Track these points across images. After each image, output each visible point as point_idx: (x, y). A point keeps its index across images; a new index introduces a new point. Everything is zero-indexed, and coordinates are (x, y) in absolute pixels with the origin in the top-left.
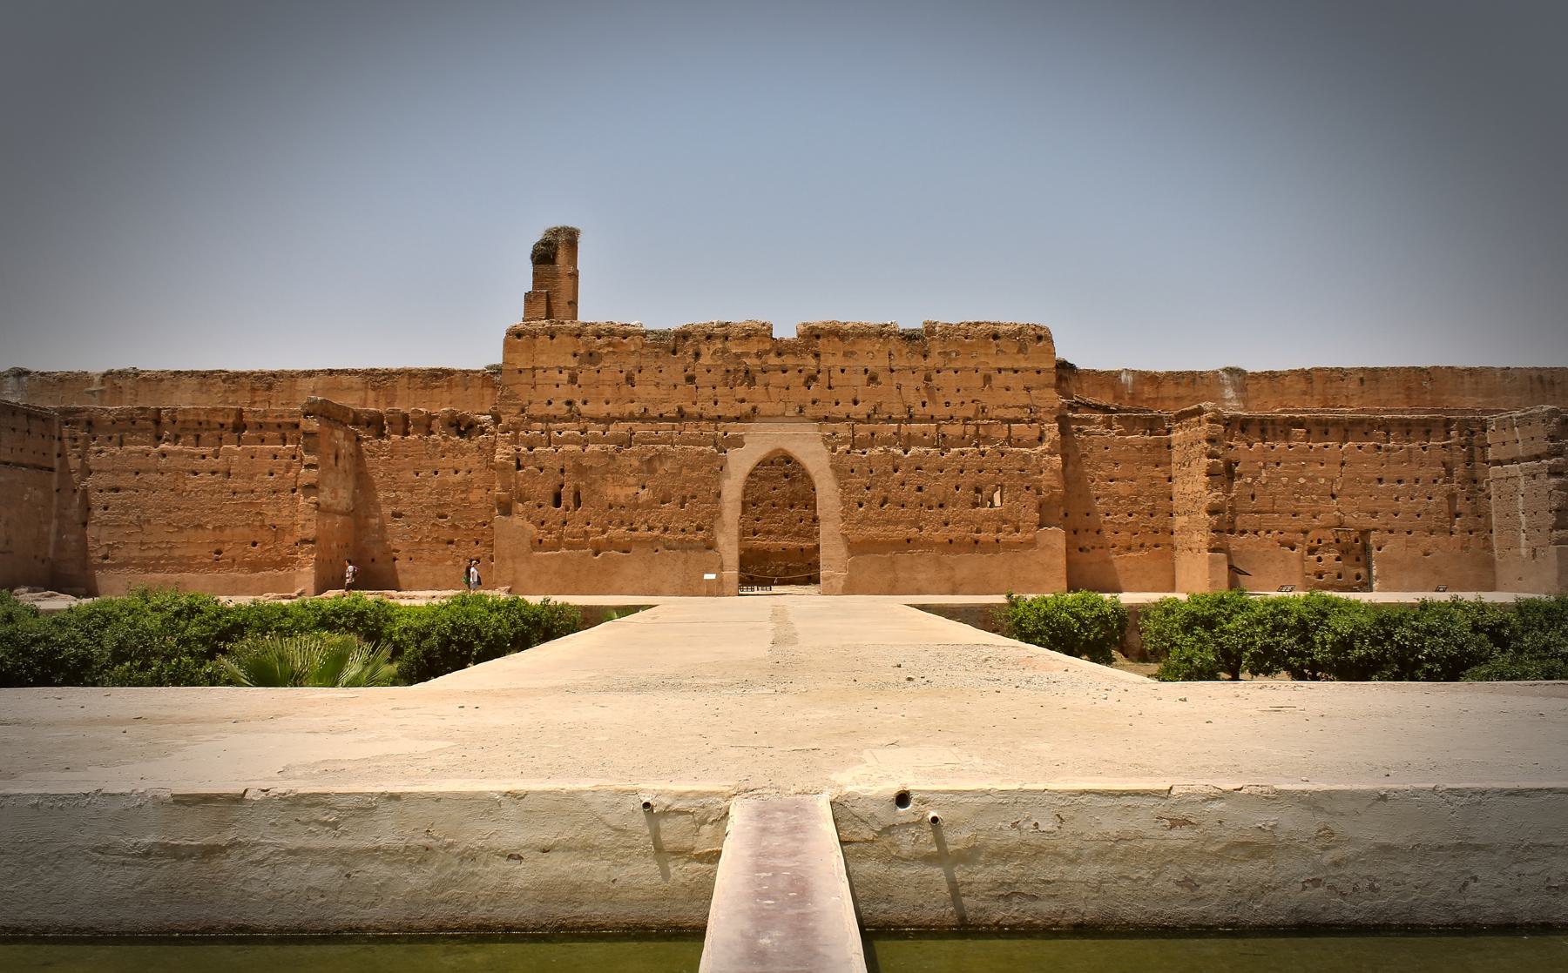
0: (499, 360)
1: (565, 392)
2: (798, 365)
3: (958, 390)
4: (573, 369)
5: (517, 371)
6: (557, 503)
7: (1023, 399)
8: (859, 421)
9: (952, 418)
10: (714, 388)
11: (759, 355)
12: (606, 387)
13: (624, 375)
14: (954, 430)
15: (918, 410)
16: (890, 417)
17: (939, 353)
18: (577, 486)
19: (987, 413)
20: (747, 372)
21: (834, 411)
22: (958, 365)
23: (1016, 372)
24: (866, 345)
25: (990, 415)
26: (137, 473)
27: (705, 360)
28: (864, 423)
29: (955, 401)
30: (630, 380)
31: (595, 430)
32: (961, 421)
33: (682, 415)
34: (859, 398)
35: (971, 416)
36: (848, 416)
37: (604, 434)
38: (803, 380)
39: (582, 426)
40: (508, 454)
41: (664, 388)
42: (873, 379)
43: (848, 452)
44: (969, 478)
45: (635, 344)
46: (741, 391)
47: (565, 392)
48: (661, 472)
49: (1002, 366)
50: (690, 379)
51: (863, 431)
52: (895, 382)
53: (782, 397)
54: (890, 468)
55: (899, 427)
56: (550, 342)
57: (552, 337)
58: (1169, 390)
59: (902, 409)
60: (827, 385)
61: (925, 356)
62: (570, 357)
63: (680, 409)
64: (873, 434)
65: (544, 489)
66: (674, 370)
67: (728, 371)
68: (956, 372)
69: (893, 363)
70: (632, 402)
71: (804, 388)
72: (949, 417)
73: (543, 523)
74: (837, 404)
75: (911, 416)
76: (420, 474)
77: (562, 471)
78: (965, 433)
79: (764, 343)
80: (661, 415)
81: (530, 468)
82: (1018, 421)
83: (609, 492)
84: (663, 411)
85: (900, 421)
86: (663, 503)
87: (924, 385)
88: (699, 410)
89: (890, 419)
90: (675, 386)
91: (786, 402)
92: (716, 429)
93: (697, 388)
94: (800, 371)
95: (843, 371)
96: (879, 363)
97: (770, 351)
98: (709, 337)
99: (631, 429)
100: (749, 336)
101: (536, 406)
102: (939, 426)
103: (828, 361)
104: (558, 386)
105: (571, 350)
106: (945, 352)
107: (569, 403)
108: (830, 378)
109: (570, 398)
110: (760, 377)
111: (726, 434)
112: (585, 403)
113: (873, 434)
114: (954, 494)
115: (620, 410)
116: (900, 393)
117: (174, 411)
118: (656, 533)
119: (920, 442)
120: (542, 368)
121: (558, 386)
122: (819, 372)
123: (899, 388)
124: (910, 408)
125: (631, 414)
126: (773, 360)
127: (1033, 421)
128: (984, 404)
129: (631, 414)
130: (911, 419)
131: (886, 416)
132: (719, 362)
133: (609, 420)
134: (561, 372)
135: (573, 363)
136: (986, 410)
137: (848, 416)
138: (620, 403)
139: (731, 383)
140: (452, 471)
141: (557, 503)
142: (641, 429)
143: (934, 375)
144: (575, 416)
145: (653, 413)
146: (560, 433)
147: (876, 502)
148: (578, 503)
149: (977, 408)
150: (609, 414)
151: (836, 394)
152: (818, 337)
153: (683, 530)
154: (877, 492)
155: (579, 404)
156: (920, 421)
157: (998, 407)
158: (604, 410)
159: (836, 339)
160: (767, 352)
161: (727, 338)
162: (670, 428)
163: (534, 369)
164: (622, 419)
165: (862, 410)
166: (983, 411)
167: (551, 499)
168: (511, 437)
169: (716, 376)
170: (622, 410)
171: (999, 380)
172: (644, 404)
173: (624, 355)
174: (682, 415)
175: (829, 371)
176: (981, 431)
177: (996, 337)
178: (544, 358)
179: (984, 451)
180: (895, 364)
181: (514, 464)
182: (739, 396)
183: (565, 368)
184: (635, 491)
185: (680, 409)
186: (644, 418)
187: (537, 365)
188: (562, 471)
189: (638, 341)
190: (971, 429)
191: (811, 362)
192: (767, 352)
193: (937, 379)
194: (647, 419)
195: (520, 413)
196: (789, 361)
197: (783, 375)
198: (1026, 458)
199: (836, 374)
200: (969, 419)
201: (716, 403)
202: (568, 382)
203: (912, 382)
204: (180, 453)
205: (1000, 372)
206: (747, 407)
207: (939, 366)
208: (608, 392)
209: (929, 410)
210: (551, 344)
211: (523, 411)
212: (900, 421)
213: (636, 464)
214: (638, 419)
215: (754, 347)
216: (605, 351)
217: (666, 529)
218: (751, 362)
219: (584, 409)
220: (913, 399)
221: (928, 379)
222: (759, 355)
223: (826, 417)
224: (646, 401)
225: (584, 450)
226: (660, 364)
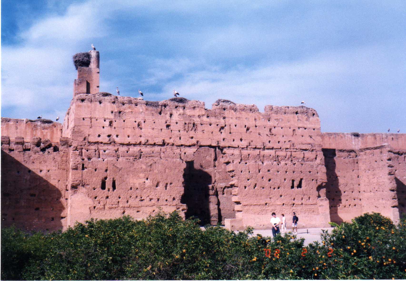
1: (107, 130)
3: (283, 136)
6: (103, 187)
7: (309, 140)
9: (281, 148)
10: (179, 131)
11: (199, 116)
13: (137, 123)
16: (256, 147)
20: (194, 124)
21: (233, 144)
22: (283, 125)
23: (305, 129)
27: (176, 117)
33: (164, 144)
35: (289, 147)
36: (238, 147)
37: (127, 152)
38: (219, 129)
39: (116, 148)
41: (157, 130)
42: (248, 129)
46: (192, 133)
47: (107, 130)
48: (156, 171)
50: (168, 126)
53: (210, 137)
57: (100, 103)
58: (327, 139)
59: (261, 144)
60: (229, 132)
61: (269, 120)
62: (110, 112)
63: (164, 140)
65: (97, 181)
66: (161, 120)
67: (185, 124)
68: (282, 128)
71: (219, 133)
72: (279, 148)
73: (96, 198)
74: (234, 140)
75: (264, 147)
77: (106, 170)
80: (155, 143)
81: (90, 169)
82: (306, 150)
83: (131, 181)
88: (173, 142)
90: (161, 130)
93: (171, 131)
94: (217, 125)
95: (236, 126)
96: (251, 123)
97: (203, 115)
99: (140, 150)
100: (194, 108)
101: (92, 137)
103: (229, 121)
104: (103, 127)
106: (277, 119)
110: (200, 128)
111: (185, 153)
112: (117, 136)
113: (249, 155)
115: (135, 141)
118: (153, 201)
120: (95, 118)
121: (103, 127)
122: (225, 126)
123: (259, 134)
126: (205, 119)
127: (313, 150)
129: (140, 142)
130: (264, 149)
131: (254, 147)
132: (182, 119)
133: (129, 144)
134: (105, 121)
135: (112, 116)
137: (238, 147)
139: (187, 129)
141: (103, 187)
142: (146, 150)
144: (112, 143)
145: (151, 142)
146: (105, 151)
147: (253, 186)
148: (114, 187)
150: (129, 142)
152: (224, 109)
153: (167, 200)
154: (252, 182)
155: (114, 137)
156: (268, 149)
158: (127, 140)
159: (233, 111)
161: (184, 108)
164: (135, 145)
165: (244, 144)
167: (99, 186)
169: (180, 126)
170: (136, 141)
172: (147, 138)
174: (164, 144)
175: (230, 125)
179: (295, 164)
182: (191, 136)
183: (107, 119)
184: (144, 181)
185: (164, 140)
187: (92, 116)
188: (106, 170)
190: (289, 154)
191: (222, 121)
193: (273, 131)
194: (148, 145)
196: (213, 120)
198: (312, 166)
199: (233, 126)
200: (287, 149)
201: (180, 139)
205: (299, 129)
206: (194, 141)
207: (276, 125)
208: (129, 131)
211: (85, 139)
213: (144, 167)
215: (197, 112)
216: (128, 111)
217: (158, 200)
218: (197, 120)
219: (117, 140)
222: (199, 116)
223: (229, 147)
225: (117, 160)
226: (154, 119)
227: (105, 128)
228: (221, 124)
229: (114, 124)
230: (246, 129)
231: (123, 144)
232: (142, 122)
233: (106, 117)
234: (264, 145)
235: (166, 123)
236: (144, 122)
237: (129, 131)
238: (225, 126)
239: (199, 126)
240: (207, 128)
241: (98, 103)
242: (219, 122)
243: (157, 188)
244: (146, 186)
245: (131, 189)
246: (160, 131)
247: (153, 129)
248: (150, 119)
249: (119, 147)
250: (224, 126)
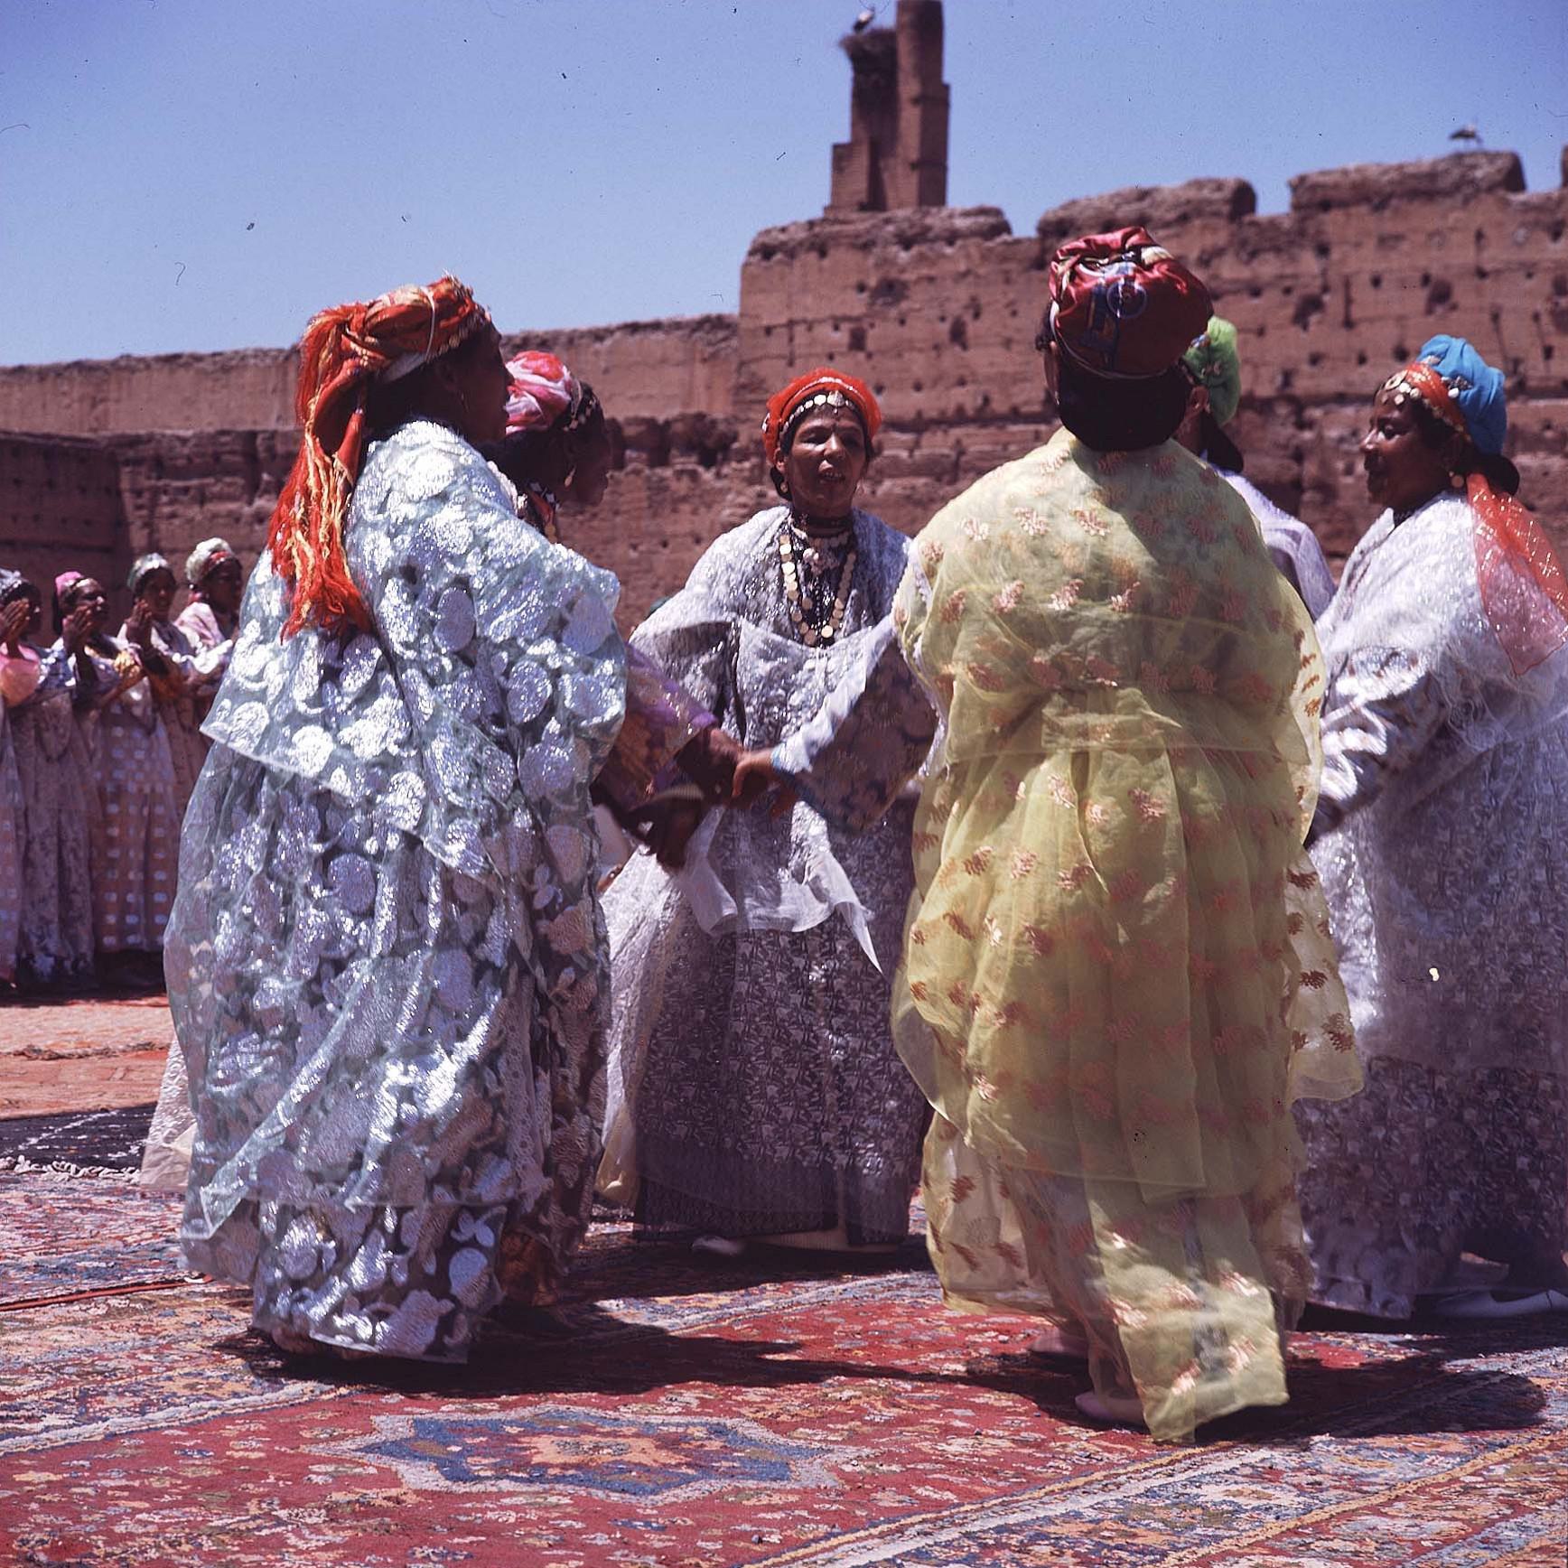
0: (727, 303)
2: (1282, 277)
4: (858, 319)
5: (762, 333)
12: (916, 355)
15: (1536, 369)
24: (1425, 217)
30: (958, 334)
40: (744, 506)
45: (968, 256)
57: (823, 253)
60: (1341, 318)
69: (1486, 255)
70: (962, 382)
84: (1018, 400)
87: (1549, 306)
91: (1256, 366)
94: (1288, 291)
100: (1184, 219)
105: (854, 280)
116: (1498, 330)
120: (804, 321)
122: (1326, 289)
124: (1517, 362)
125: (960, 410)
129: (960, 410)
133: (918, 425)
135: (856, 304)
138: (940, 388)
145: (999, 406)
160: (1219, 252)
162: (1030, 436)
163: (791, 324)
168: (752, 469)
170: (942, 404)
173: (949, 283)
178: (809, 300)
180: (1493, 256)
189: (974, 251)
191: (1309, 263)
192: (1219, 252)
196: (1268, 267)
197: (1256, 301)
199: (1362, 291)
208: (918, 364)
210: (821, 270)
224: (989, 379)
225: (873, 492)
226: (1011, 296)
228: (1306, 286)
229: (873, 339)
230: (1422, 295)
232: (968, 318)
233: (839, 312)
234: (1515, 372)
237: (918, 364)
238: (1326, 289)
241: (812, 257)
247: (1008, 343)
248: (993, 297)
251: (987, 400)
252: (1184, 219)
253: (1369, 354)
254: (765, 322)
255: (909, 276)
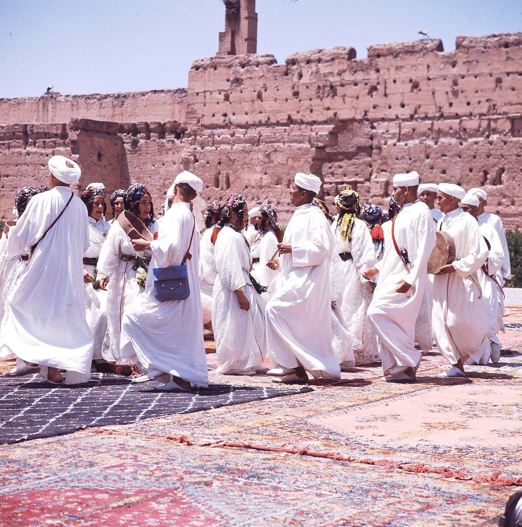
2: (364, 80)
4: (227, 91)
5: (195, 94)
8: (404, 120)
12: (246, 103)
14: (472, 124)
15: (447, 111)
17: (464, 63)
18: (227, 174)
19: (497, 110)
22: (477, 72)
24: (411, 60)
25: (498, 112)
26: (16, 166)
27: (305, 79)
28: (408, 121)
29: (474, 101)
30: (259, 96)
31: (240, 133)
32: (478, 117)
33: (290, 121)
34: (405, 102)
38: (367, 91)
39: (231, 131)
40: (190, 152)
42: (415, 86)
43: (395, 145)
44: (478, 164)
45: (263, 71)
46: (327, 102)
47: (224, 107)
48: (276, 163)
49: (509, 70)
51: (407, 127)
52: (431, 88)
53: (354, 105)
54: (423, 156)
55: (432, 124)
56: (213, 72)
57: (215, 69)
60: (383, 93)
63: (289, 117)
64: (414, 130)
69: (431, 72)
70: (261, 113)
76: (155, 166)
77: (220, 163)
78: (480, 126)
79: (343, 63)
80: (278, 122)
84: (279, 119)
85: (433, 118)
86: (277, 184)
87: (451, 89)
88: (301, 117)
89: (426, 118)
91: (356, 109)
92: (311, 130)
94: (366, 84)
95: (395, 82)
96: (419, 74)
98: (308, 62)
100: (333, 59)
102: (460, 123)
105: (226, 78)
106: (468, 62)
107: (225, 115)
108: (386, 88)
109: (225, 112)
113: (414, 130)
114: (467, 175)
116: (434, 98)
117: (33, 126)
119: (446, 134)
120: (209, 91)
121: (218, 103)
122: (378, 84)
124: (440, 108)
125: (260, 121)
128: (495, 103)
129: (260, 121)
130: (442, 116)
131: (423, 116)
132: (314, 81)
133: (247, 126)
135: (227, 86)
136: (496, 107)
138: (254, 114)
140: (172, 163)
142: (266, 132)
143: (460, 81)
145: (273, 120)
148: (228, 186)
149: (490, 106)
151: (391, 100)
155: (230, 116)
157: (506, 104)
160: (344, 71)
162: (283, 131)
165: (407, 112)
166: (494, 108)
168: (192, 140)
169: (313, 91)
170: (255, 119)
171: (507, 81)
173: (257, 79)
174: (290, 121)
176: (493, 125)
177: (506, 45)
178: (211, 84)
181: (192, 158)
182: (326, 106)
185: (289, 117)
186: (268, 124)
189: (264, 69)
190: (484, 124)
191: (373, 75)
195: (197, 124)
196: (360, 76)
197: (356, 87)
199: (390, 84)
200: (485, 115)
202: (225, 100)
203: (445, 86)
204: (36, 153)
207: (463, 73)
208: (247, 106)
209: (454, 110)
210: (215, 74)
211: (199, 122)
212: (433, 118)
213: (261, 157)
214: (264, 125)
216: (245, 78)
217: (278, 203)
218: (335, 79)
219: (233, 119)
220: (441, 99)
221: (455, 83)
222: (339, 74)
224: (269, 111)
226: (277, 84)
227: (220, 103)
228: (372, 82)
231: (240, 126)
232: (263, 91)
233: (220, 89)
234: (440, 111)
235: (293, 88)
236: (266, 90)
237: (247, 106)
239: (339, 89)
240: (351, 90)
241: (212, 69)
242: (368, 79)
243: (277, 186)
244: (263, 184)
245: (246, 187)
246: (285, 101)
247: (276, 100)
248: (271, 85)
249: (234, 130)
250: (376, 84)
251: (269, 118)
252: (333, 59)
253: (392, 105)
254: (196, 91)
255: (244, 77)
